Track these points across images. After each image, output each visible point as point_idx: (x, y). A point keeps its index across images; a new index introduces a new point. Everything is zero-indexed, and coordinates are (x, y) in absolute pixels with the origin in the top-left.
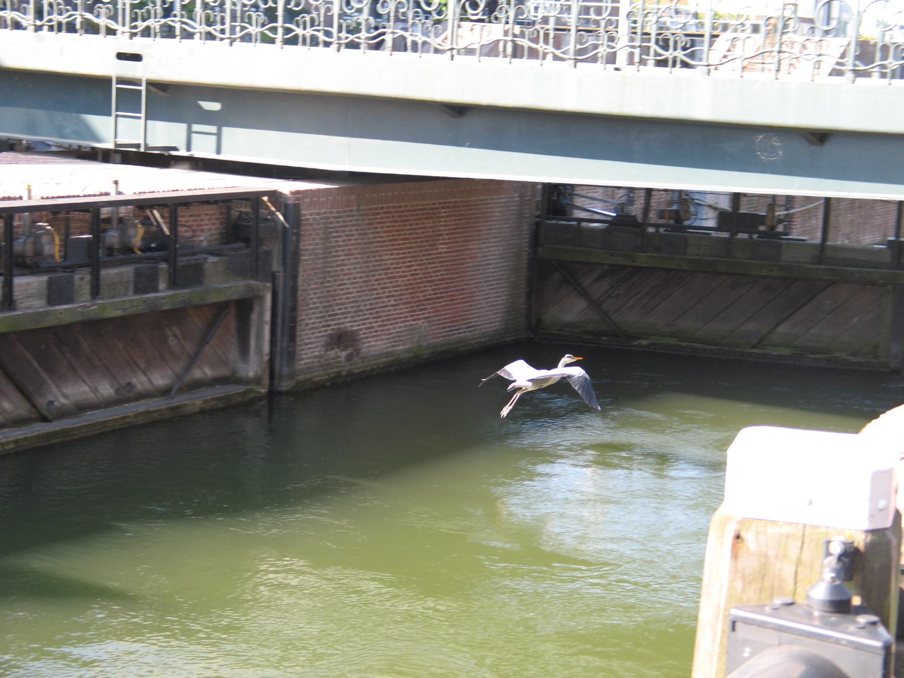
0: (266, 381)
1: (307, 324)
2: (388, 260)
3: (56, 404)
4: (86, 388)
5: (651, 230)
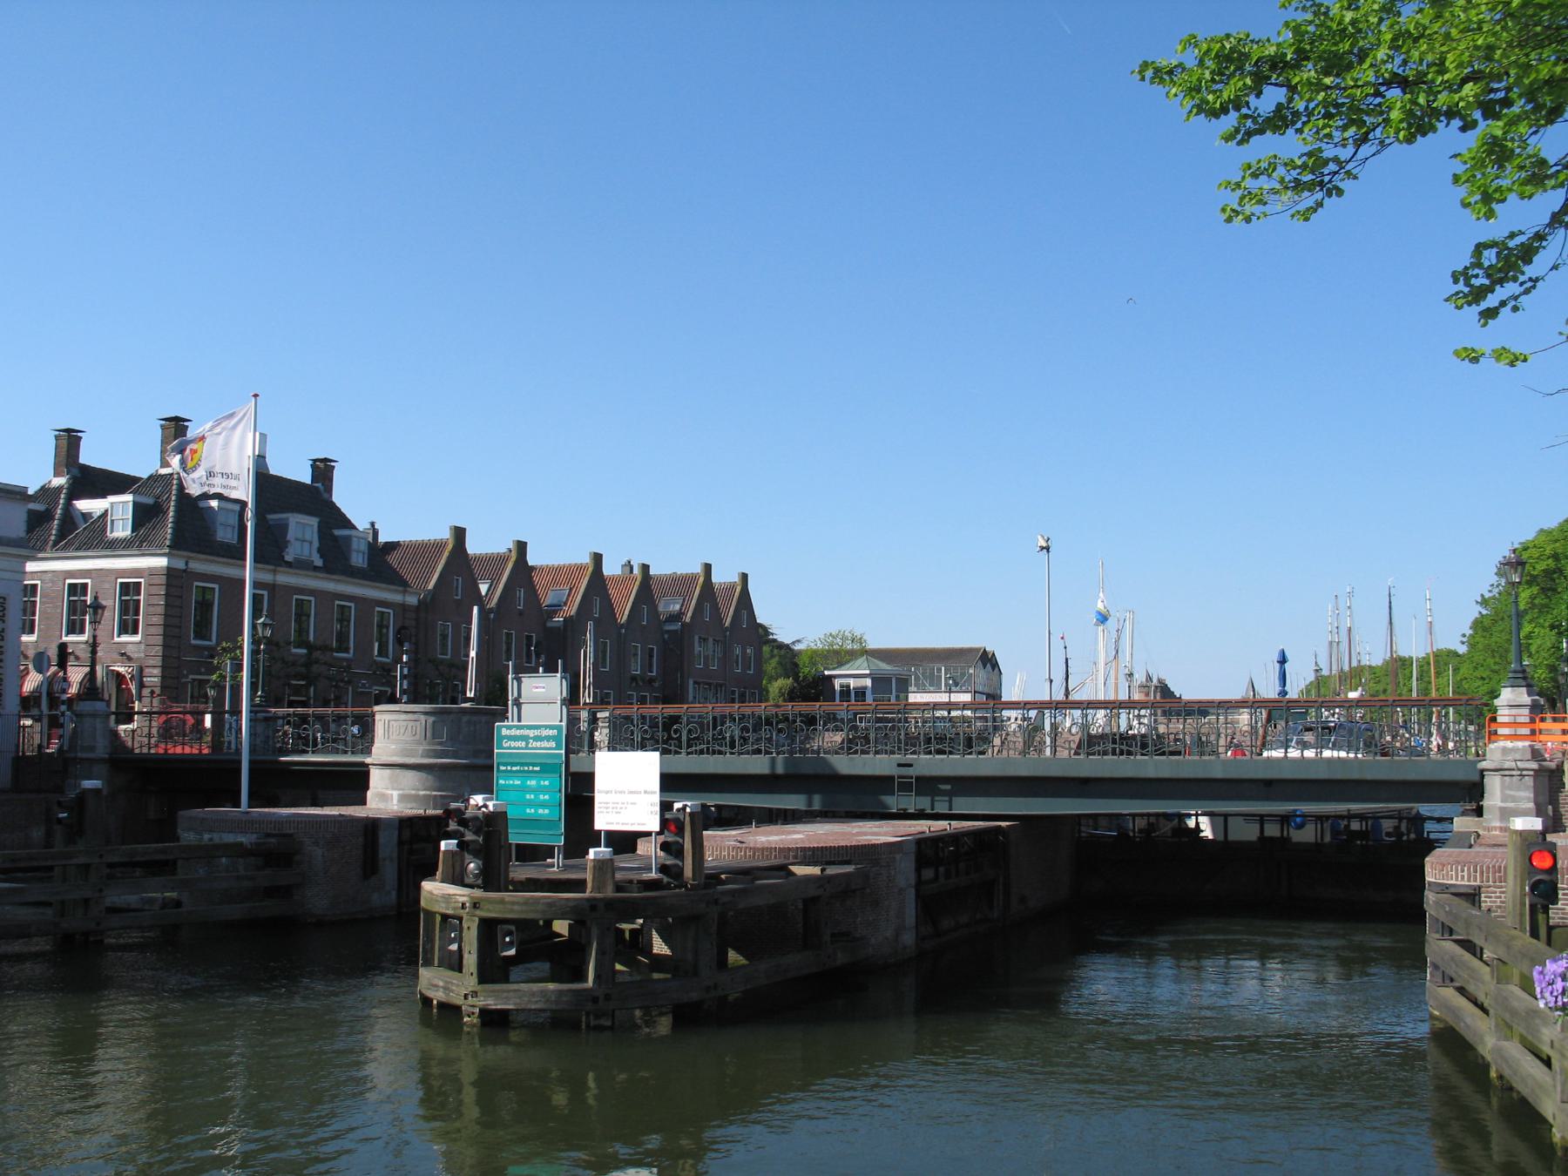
5: (1138, 839)
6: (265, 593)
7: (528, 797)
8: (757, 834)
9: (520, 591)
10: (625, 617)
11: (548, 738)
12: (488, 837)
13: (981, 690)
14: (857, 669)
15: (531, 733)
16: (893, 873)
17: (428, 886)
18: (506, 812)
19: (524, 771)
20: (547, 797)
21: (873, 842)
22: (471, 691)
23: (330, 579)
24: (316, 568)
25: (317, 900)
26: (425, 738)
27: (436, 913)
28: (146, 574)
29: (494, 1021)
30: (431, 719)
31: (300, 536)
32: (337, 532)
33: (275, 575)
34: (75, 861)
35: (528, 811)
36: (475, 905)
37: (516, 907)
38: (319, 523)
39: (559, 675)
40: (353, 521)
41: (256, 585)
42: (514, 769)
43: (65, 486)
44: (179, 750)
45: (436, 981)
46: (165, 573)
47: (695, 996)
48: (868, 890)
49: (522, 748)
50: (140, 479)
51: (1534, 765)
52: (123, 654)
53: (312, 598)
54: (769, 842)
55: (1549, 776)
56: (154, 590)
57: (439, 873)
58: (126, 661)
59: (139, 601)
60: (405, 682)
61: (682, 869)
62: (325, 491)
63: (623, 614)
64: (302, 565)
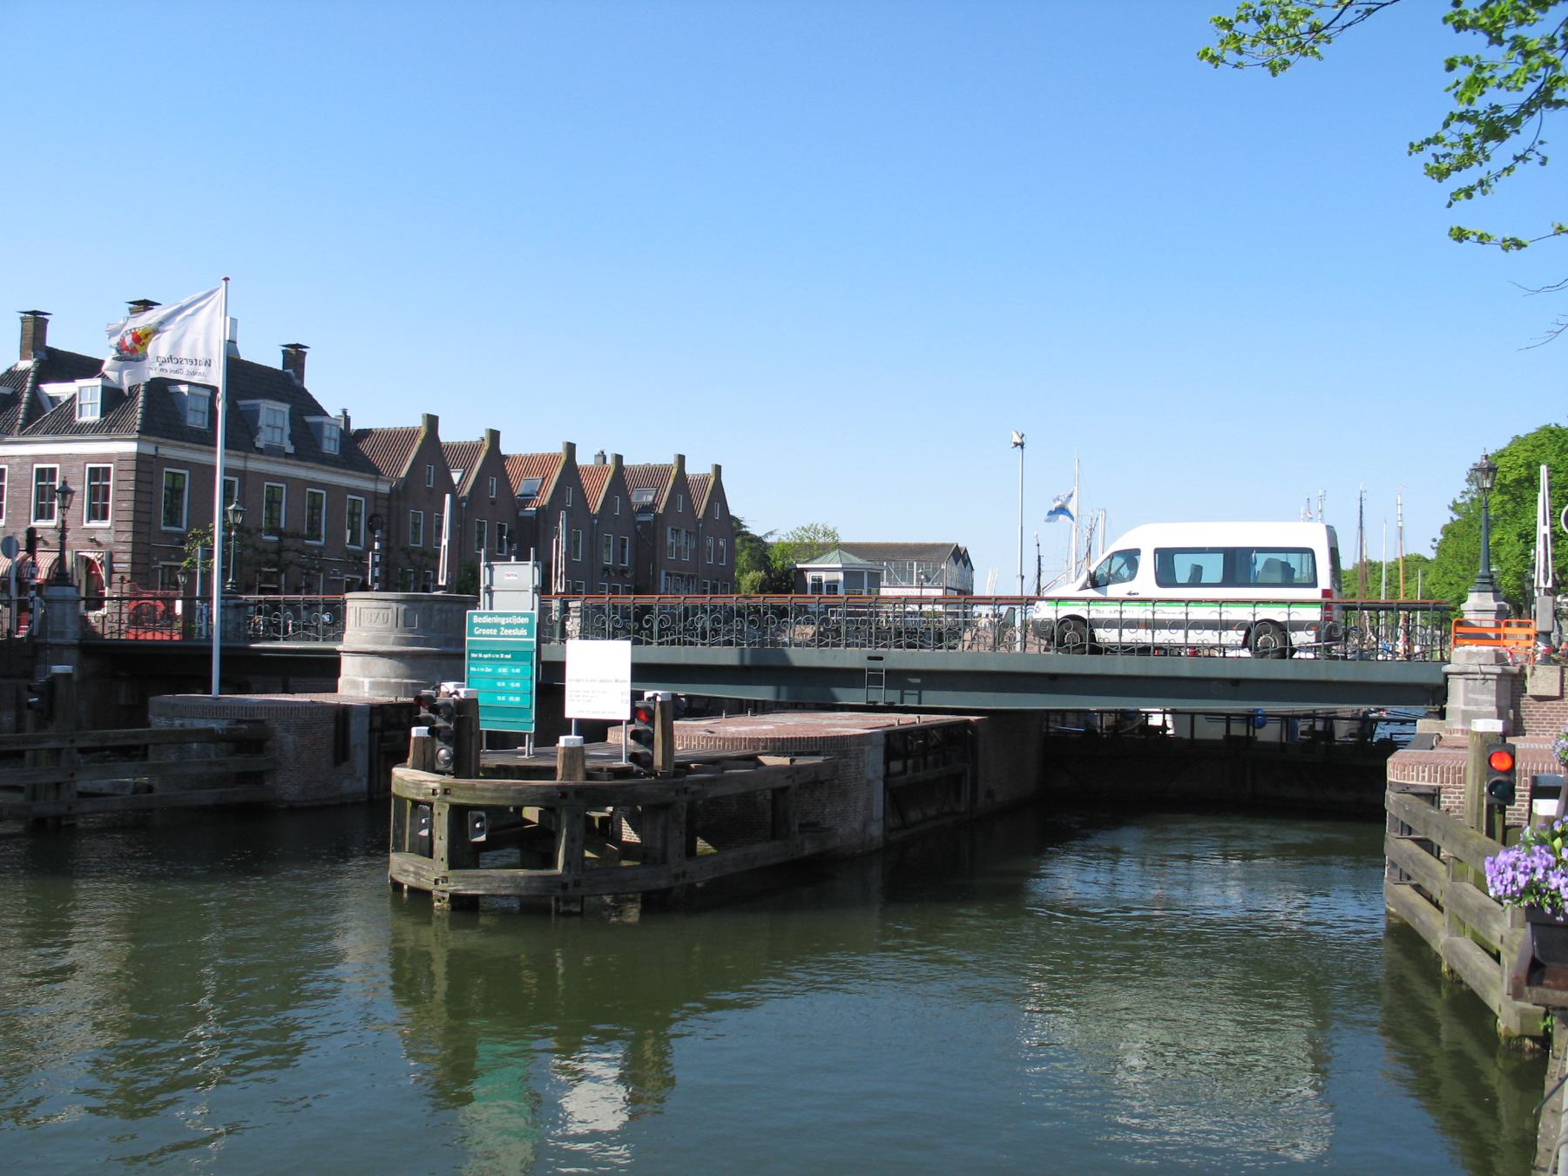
6: (236, 480)
7: (499, 684)
8: (727, 724)
10: (598, 508)
11: (519, 626)
12: (459, 722)
13: (953, 586)
15: (503, 621)
16: (861, 764)
17: (398, 772)
18: (476, 700)
19: (495, 659)
20: (518, 685)
21: (842, 734)
22: (442, 578)
24: (287, 455)
25: (288, 786)
27: (406, 799)
28: (115, 460)
29: (464, 906)
30: (403, 607)
31: (271, 423)
32: (309, 419)
34: (46, 746)
35: (499, 698)
36: (446, 792)
37: (487, 794)
39: (531, 563)
40: (325, 408)
41: (227, 471)
42: (486, 656)
43: (33, 369)
44: (149, 636)
45: (407, 867)
47: (663, 883)
48: (837, 782)
49: (493, 636)
51: (1498, 670)
52: (93, 540)
53: (283, 486)
54: (739, 732)
55: (1512, 681)
56: (123, 476)
57: (410, 760)
59: (108, 486)
60: (377, 570)
61: (652, 758)
64: (273, 452)
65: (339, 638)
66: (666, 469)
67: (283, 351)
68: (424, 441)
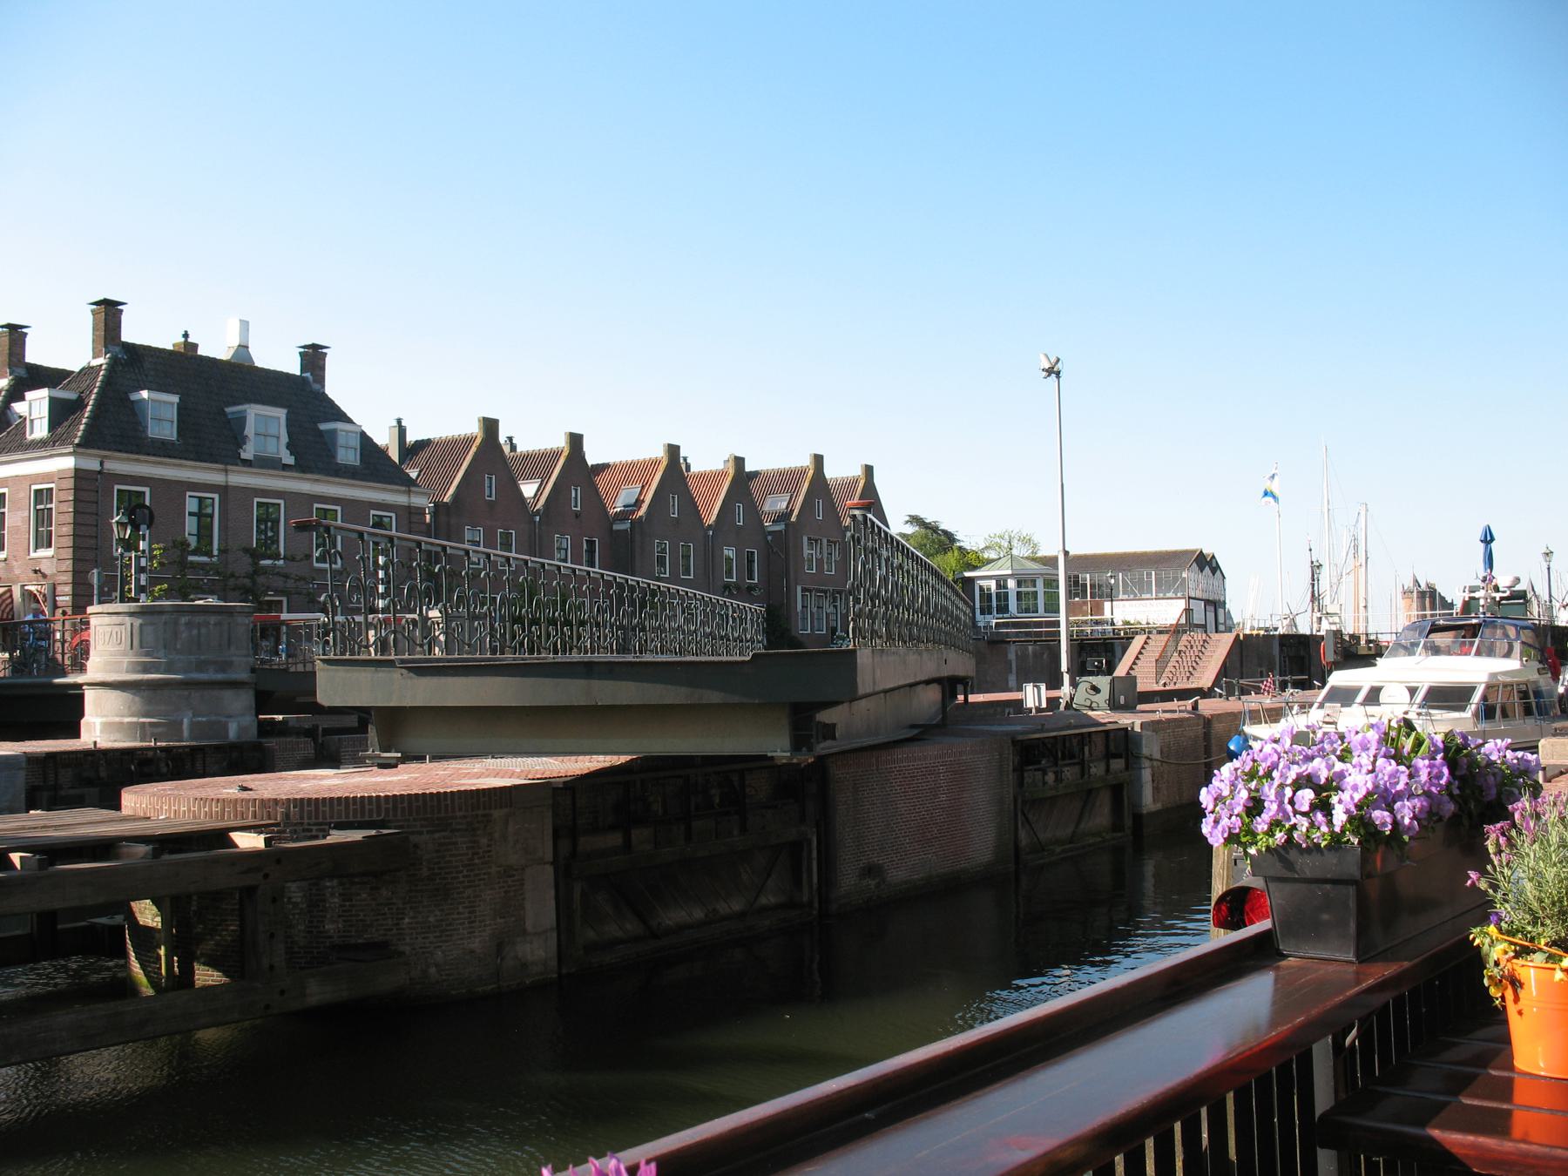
0: (816, 905)
1: (845, 860)
2: (903, 807)
3: (663, 925)
4: (683, 913)
6: (216, 496)
9: (576, 490)
10: (714, 518)
13: (1193, 596)
14: (998, 569)
16: (484, 841)
23: (308, 479)
24: (286, 467)
26: (132, 648)
28: (56, 479)
30: (138, 622)
31: (262, 431)
32: (323, 427)
33: (227, 475)
38: (287, 414)
40: (349, 415)
43: (6, 388)
46: (73, 475)
50: (73, 372)
52: (36, 572)
53: (282, 502)
54: (378, 784)
58: (41, 578)
60: (143, 577)
62: (315, 381)
63: (711, 518)
65: (82, 669)
66: (802, 472)
67: (300, 353)
68: (479, 448)
